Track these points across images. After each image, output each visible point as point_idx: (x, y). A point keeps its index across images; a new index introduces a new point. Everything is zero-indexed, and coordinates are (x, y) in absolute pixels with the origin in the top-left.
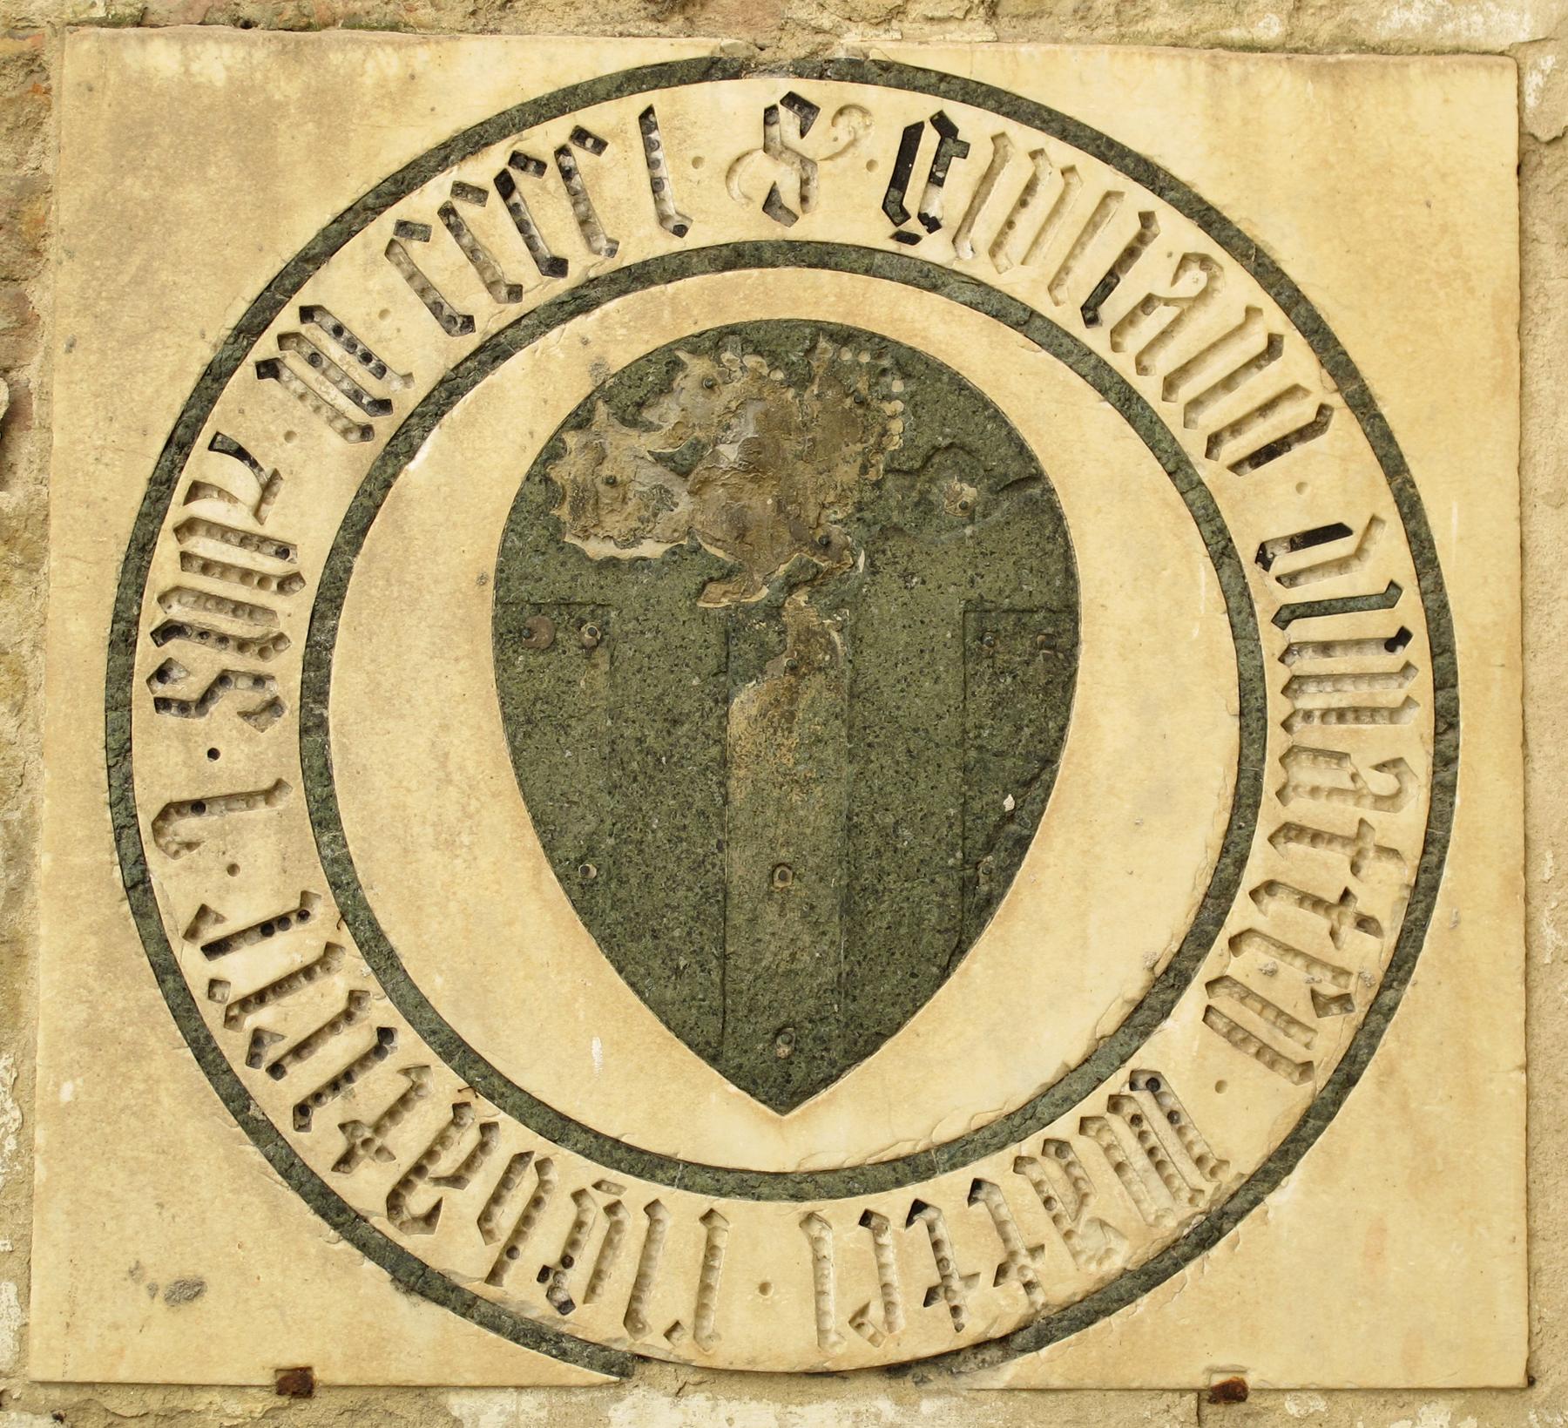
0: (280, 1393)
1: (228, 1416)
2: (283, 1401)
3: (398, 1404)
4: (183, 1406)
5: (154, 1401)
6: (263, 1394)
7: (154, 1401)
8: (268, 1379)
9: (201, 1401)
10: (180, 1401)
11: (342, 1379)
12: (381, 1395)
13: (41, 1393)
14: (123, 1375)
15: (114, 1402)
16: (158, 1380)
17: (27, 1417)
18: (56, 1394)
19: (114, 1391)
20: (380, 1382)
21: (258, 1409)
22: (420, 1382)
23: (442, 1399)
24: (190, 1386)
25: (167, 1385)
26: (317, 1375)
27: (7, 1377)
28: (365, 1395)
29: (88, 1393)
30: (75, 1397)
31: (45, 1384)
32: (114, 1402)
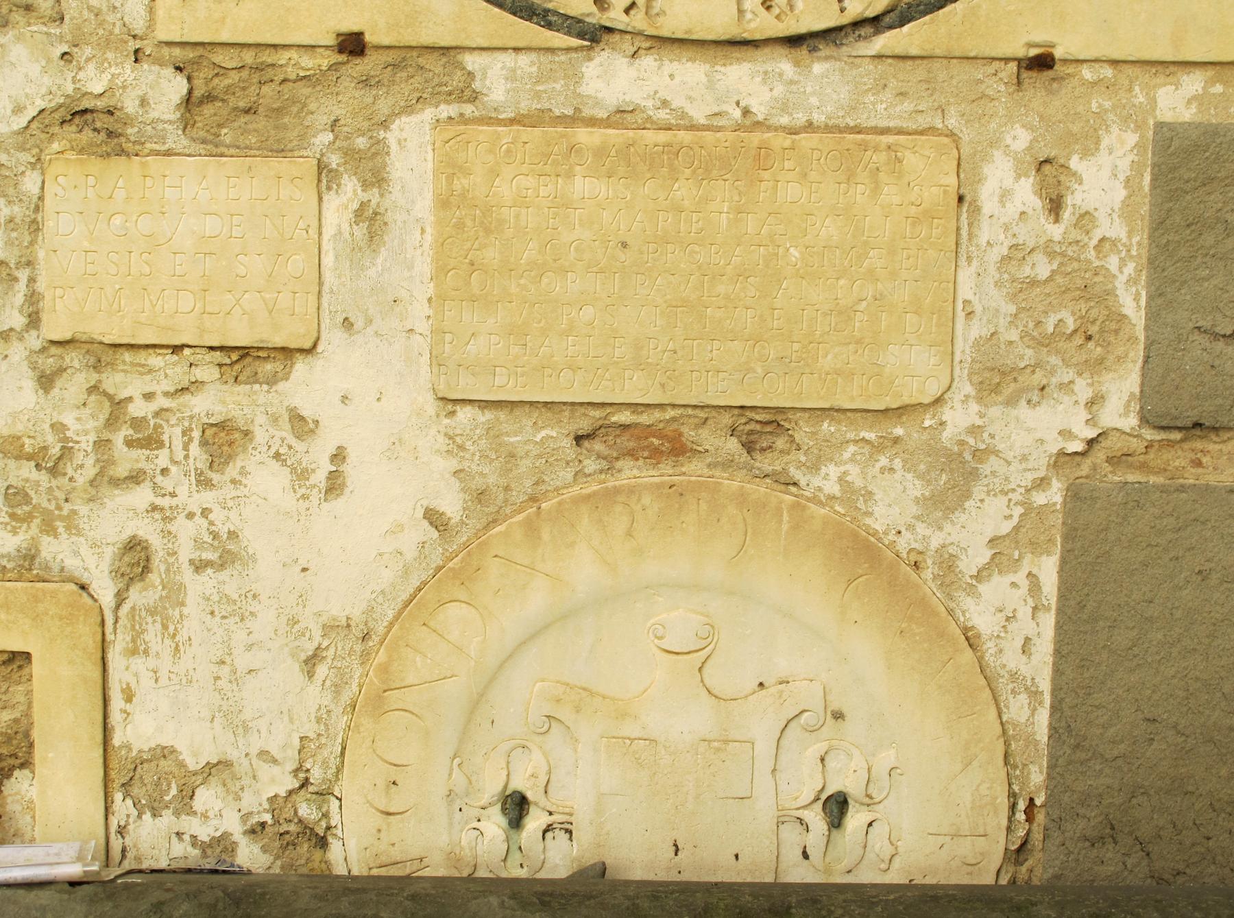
0: (341, 52)
1: (302, 68)
2: (343, 58)
3: (428, 61)
4: (270, 61)
5: (248, 57)
6: (328, 52)
7: (248, 57)
8: (331, 40)
9: (283, 57)
10: (267, 57)
11: (386, 41)
12: (415, 54)
13: (166, 51)
14: (225, 37)
15: (220, 57)
16: (251, 41)
17: (156, 68)
18: (177, 51)
19: (219, 49)
20: (414, 44)
21: (325, 64)
22: (443, 44)
23: (460, 57)
24: (275, 46)
25: (258, 45)
26: (368, 38)
27: (142, 39)
28: (402, 53)
29: (200, 51)
30: (191, 54)
31: (169, 44)
32: (220, 57)
